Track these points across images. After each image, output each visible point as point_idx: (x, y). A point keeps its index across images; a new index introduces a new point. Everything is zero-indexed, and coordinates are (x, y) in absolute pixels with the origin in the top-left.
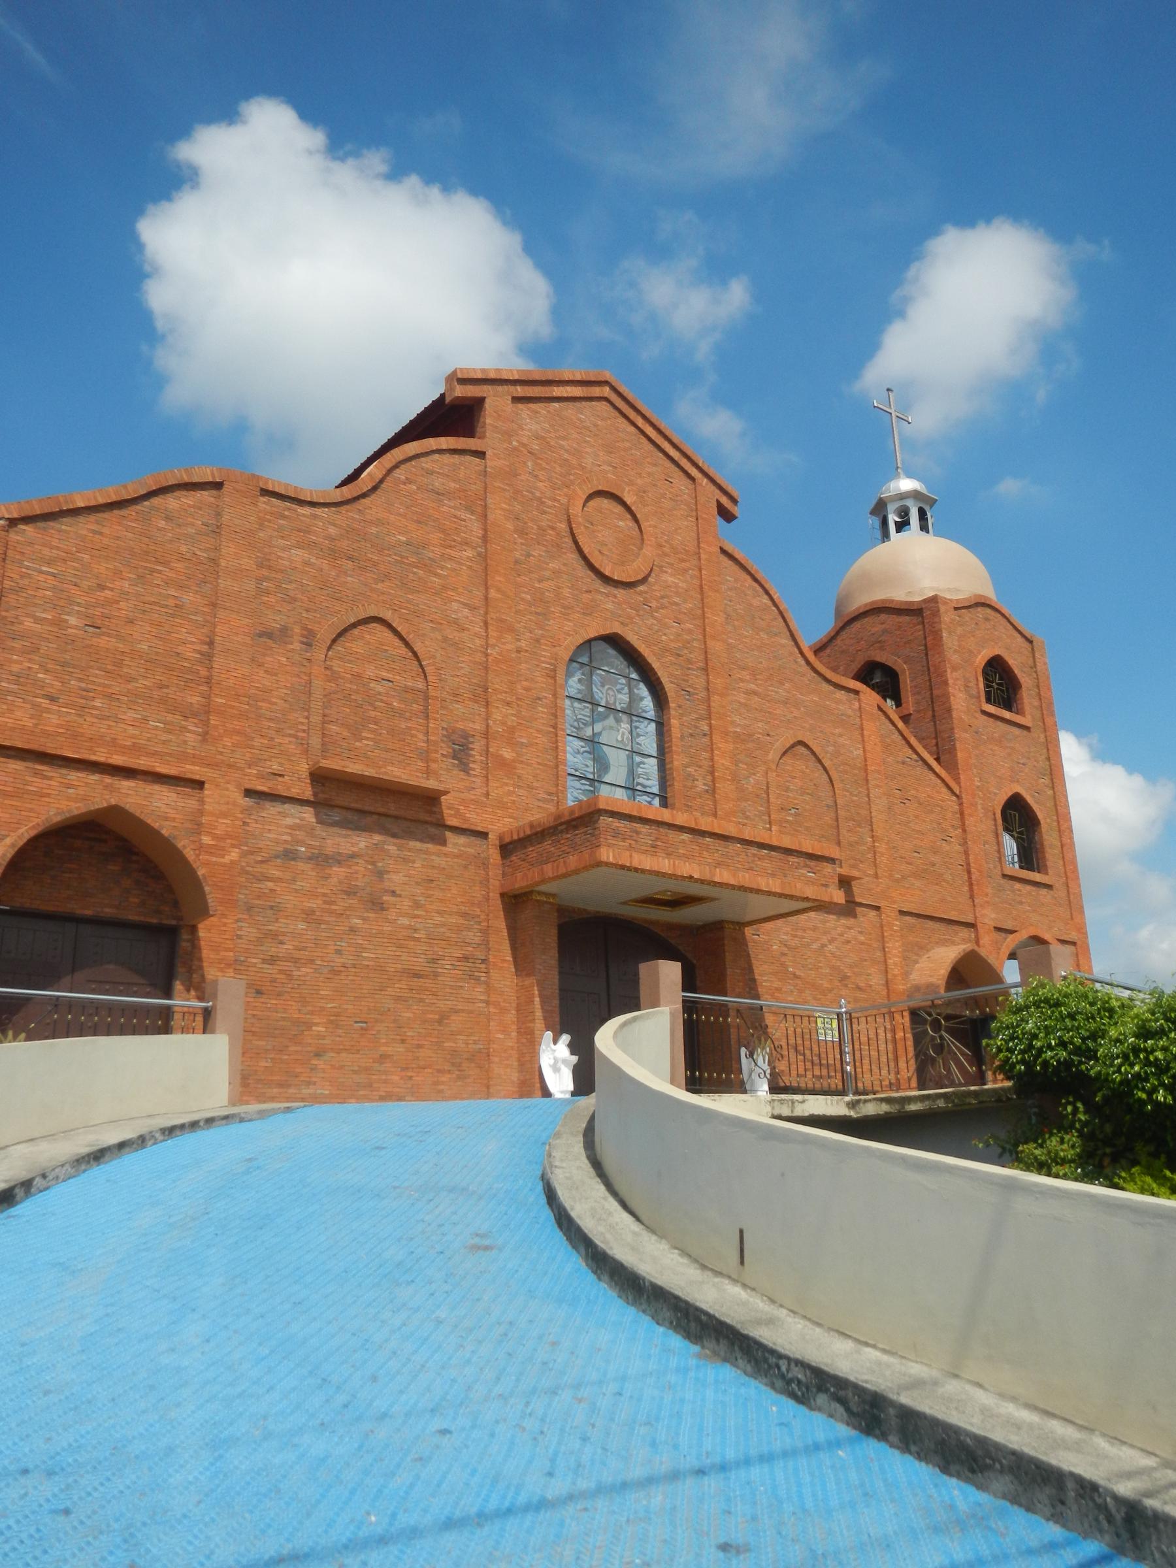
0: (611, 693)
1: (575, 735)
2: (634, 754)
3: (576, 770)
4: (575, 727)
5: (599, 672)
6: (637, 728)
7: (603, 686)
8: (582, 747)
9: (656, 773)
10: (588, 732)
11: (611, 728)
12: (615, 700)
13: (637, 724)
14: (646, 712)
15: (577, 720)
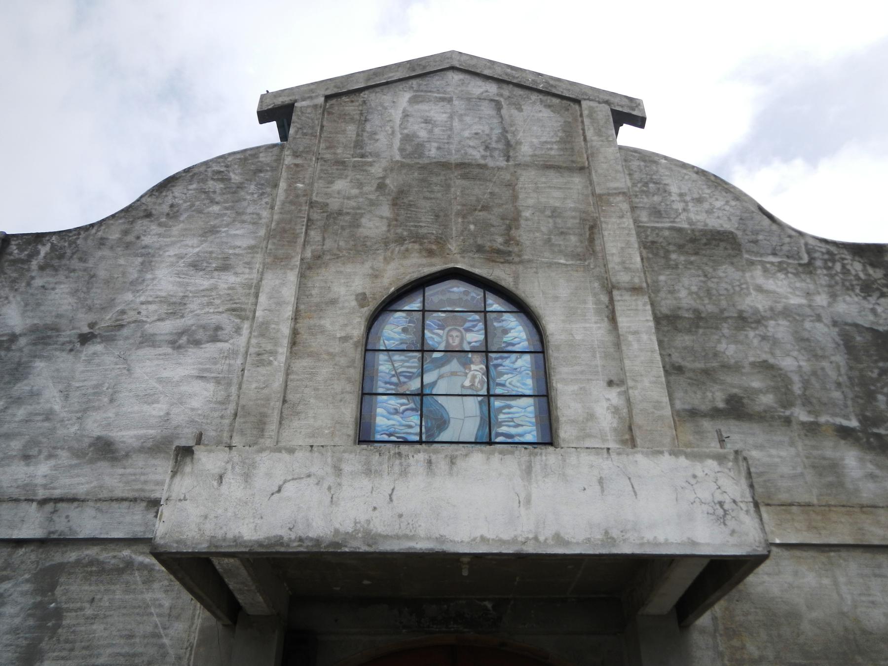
0: (455, 334)
1: (393, 392)
2: (492, 399)
3: (390, 435)
4: (391, 383)
5: (435, 314)
6: (496, 366)
7: (442, 327)
8: (402, 405)
9: (532, 415)
10: (415, 385)
11: (453, 374)
12: (462, 339)
13: (499, 361)
14: (513, 345)
15: (397, 375)
